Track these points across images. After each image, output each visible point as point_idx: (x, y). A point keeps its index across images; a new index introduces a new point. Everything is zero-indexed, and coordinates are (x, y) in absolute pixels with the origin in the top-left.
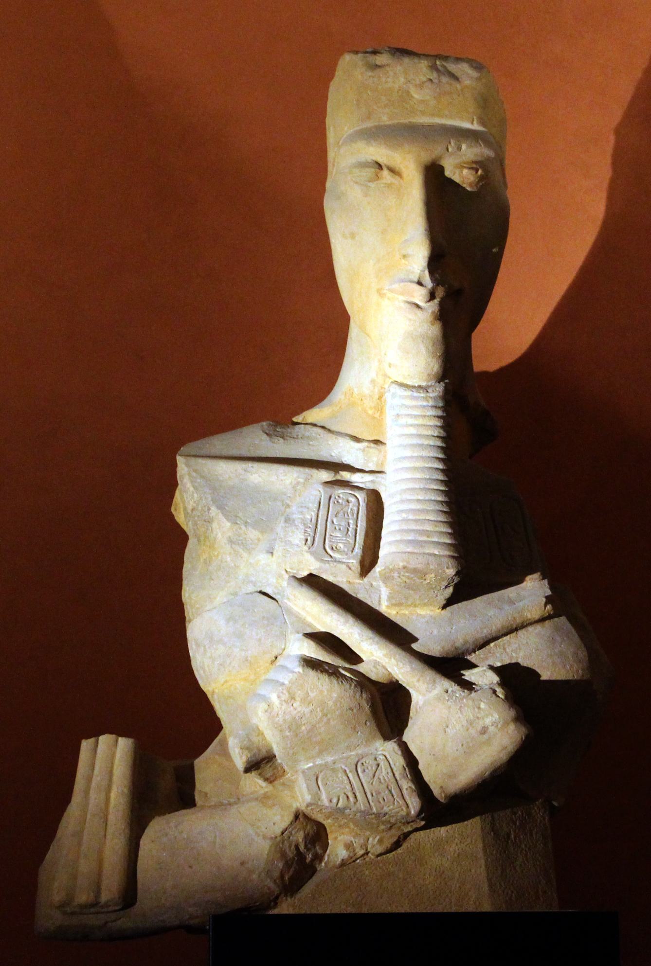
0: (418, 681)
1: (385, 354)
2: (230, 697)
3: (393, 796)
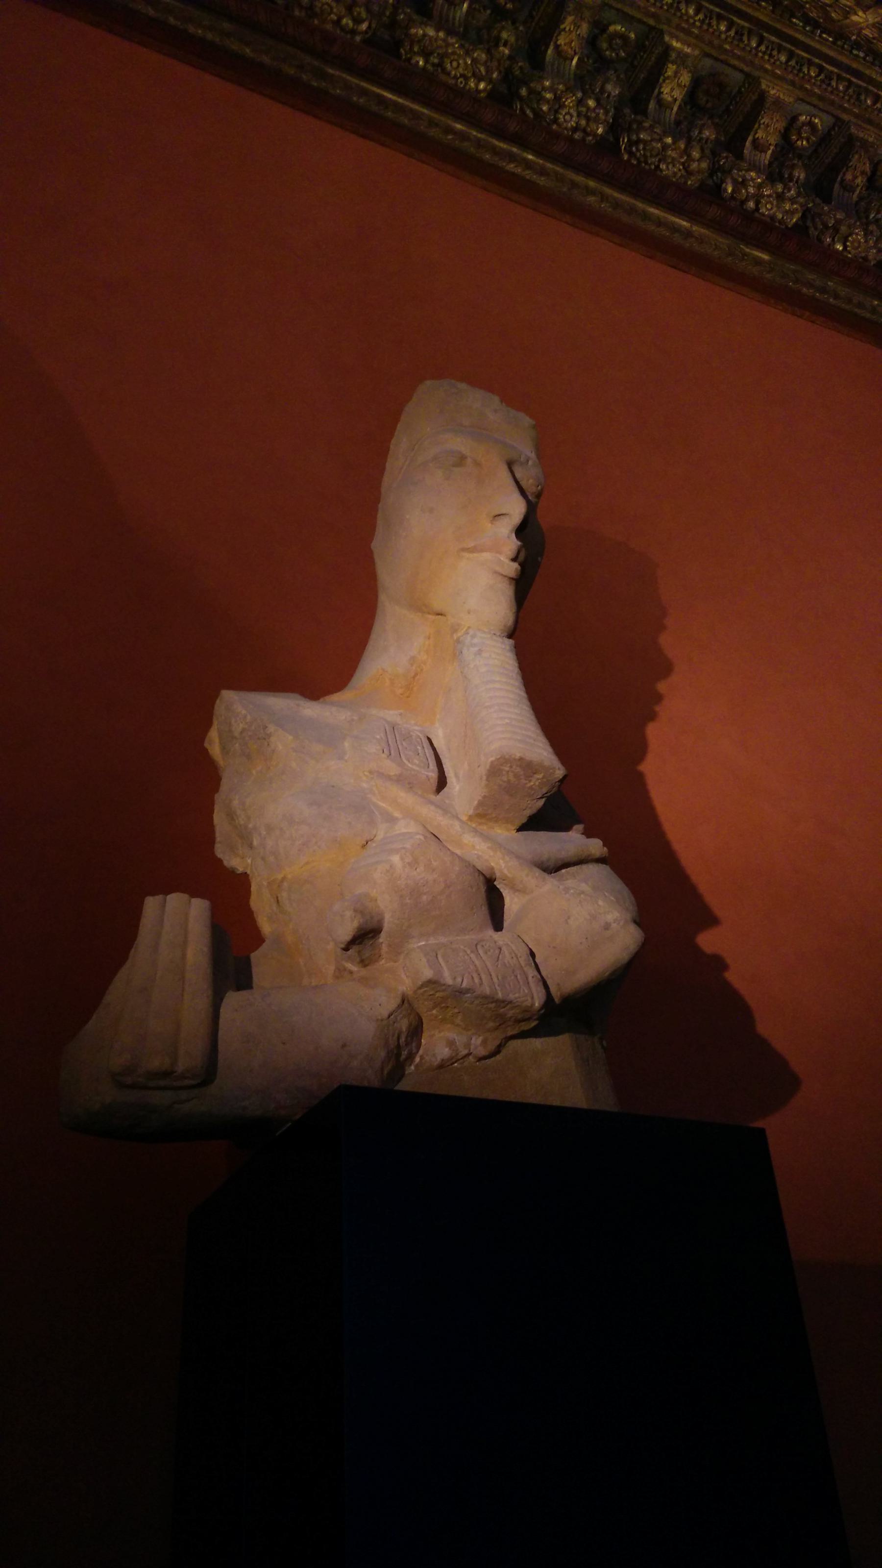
0: (527, 875)
3: (519, 982)
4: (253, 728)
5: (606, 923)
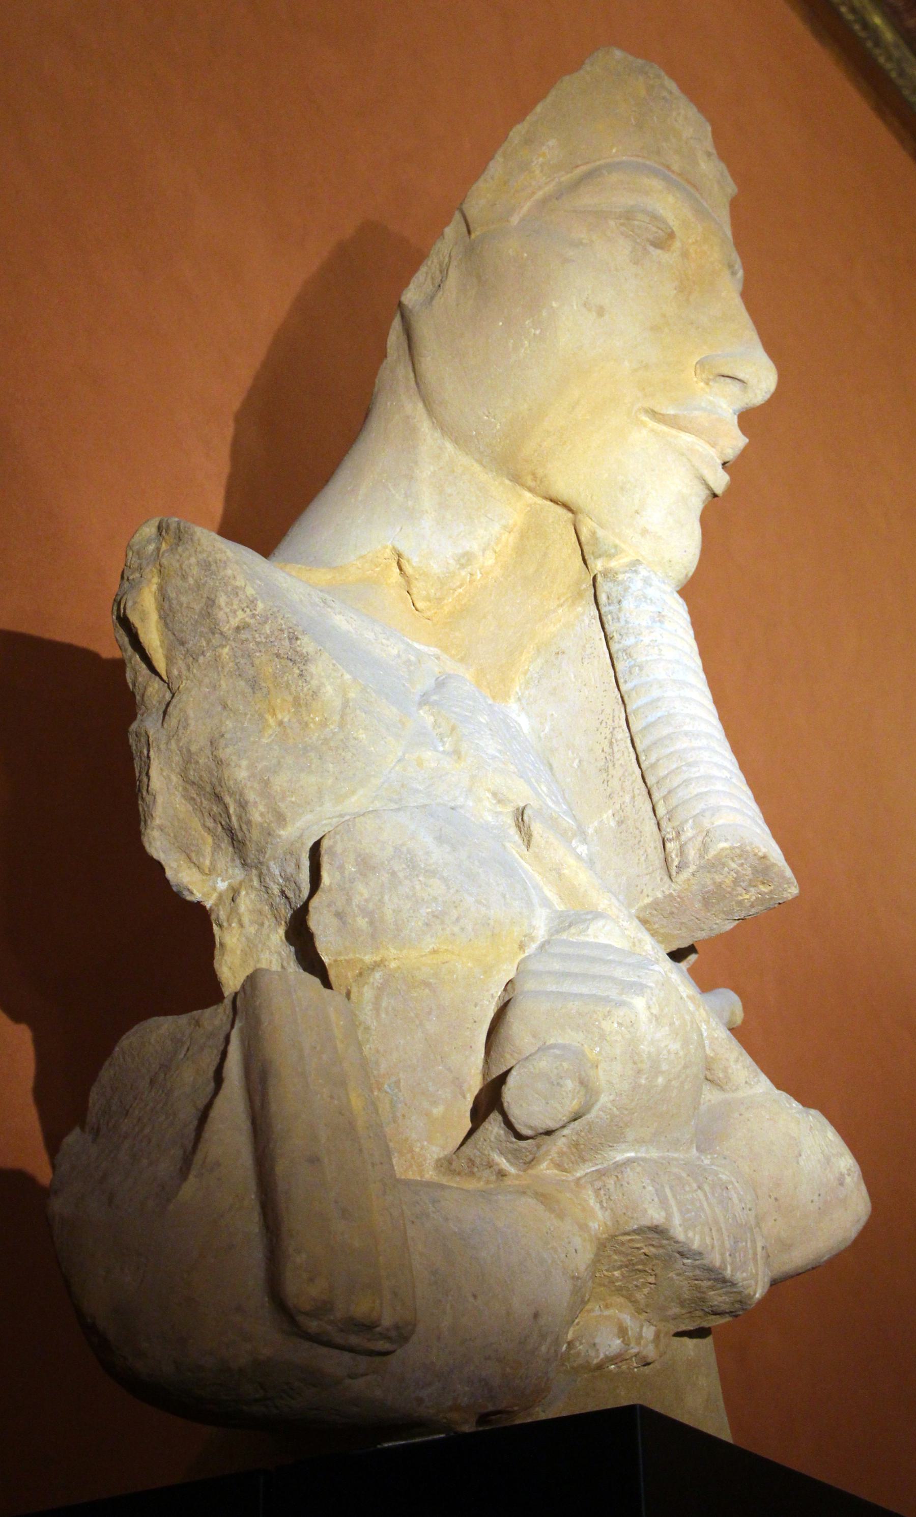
2: (427, 984)
4: (267, 629)
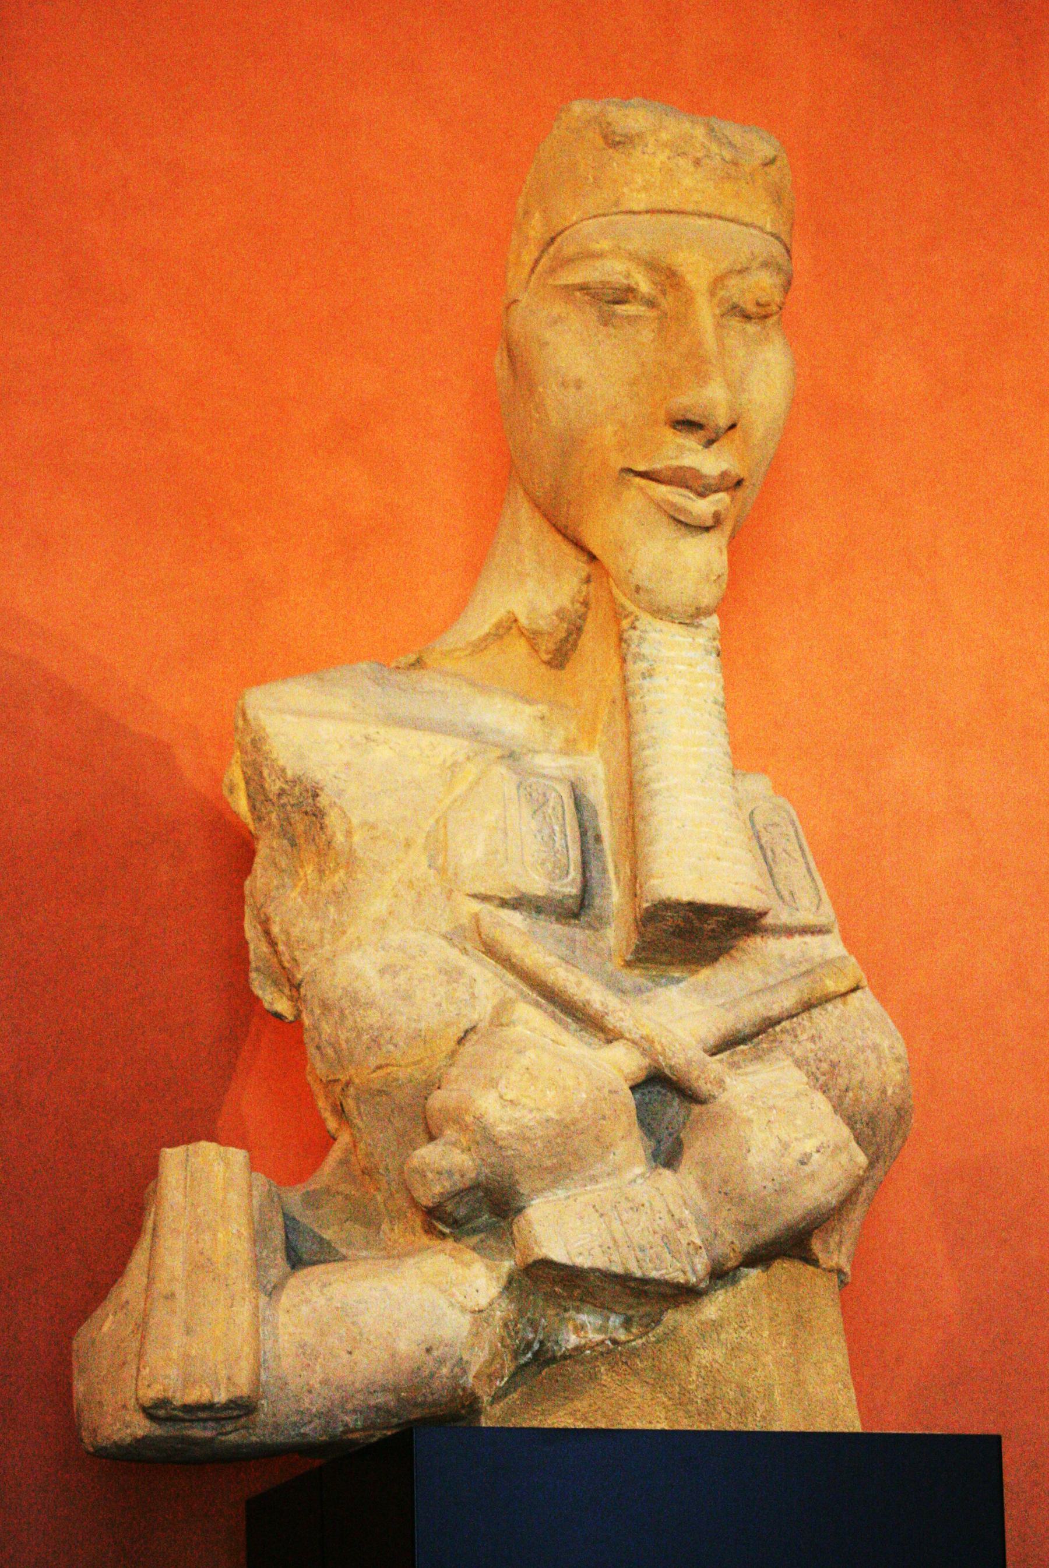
1: (630, 571)
5: (805, 1154)
